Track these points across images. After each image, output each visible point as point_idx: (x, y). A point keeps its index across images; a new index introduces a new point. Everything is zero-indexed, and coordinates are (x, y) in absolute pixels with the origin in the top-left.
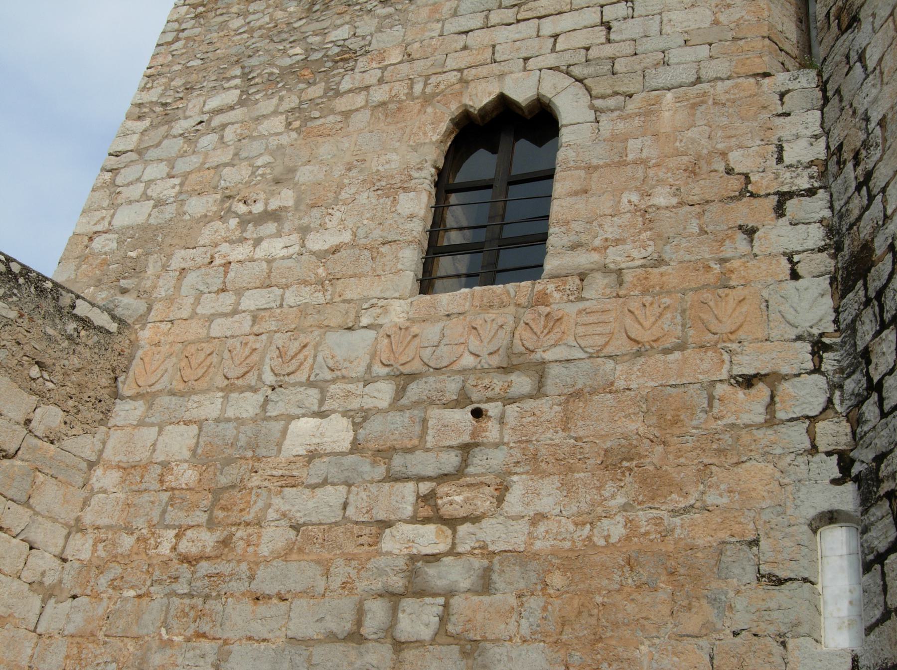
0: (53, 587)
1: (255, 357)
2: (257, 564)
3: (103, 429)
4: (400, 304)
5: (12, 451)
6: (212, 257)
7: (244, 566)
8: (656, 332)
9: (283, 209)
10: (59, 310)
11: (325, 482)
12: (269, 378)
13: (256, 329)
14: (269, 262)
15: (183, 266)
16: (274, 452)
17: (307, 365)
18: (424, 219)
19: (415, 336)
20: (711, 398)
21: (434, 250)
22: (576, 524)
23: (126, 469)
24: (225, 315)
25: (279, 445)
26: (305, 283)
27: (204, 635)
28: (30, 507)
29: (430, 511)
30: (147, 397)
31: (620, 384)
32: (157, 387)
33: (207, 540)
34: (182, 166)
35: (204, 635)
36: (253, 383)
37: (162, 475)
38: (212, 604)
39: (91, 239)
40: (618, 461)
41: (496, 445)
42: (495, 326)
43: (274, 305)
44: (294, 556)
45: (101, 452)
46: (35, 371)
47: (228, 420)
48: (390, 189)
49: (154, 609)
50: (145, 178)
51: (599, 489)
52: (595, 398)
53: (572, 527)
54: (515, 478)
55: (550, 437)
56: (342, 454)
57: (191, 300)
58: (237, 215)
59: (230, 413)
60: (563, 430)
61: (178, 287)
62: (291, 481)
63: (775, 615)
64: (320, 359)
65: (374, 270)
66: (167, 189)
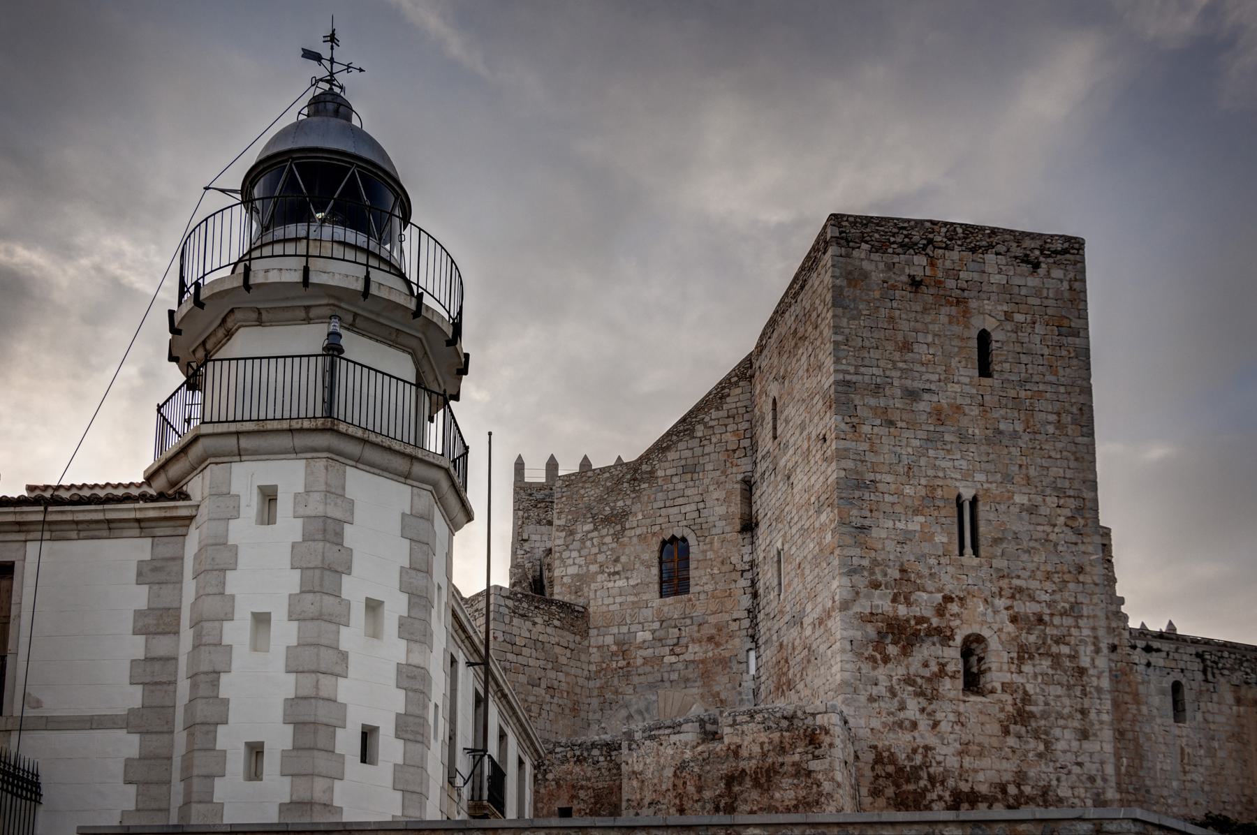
4: (657, 602)
21: (661, 582)
29: (672, 653)
30: (598, 628)
33: (622, 663)
40: (711, 639)
48: (649, 567)
55: (696, 635)
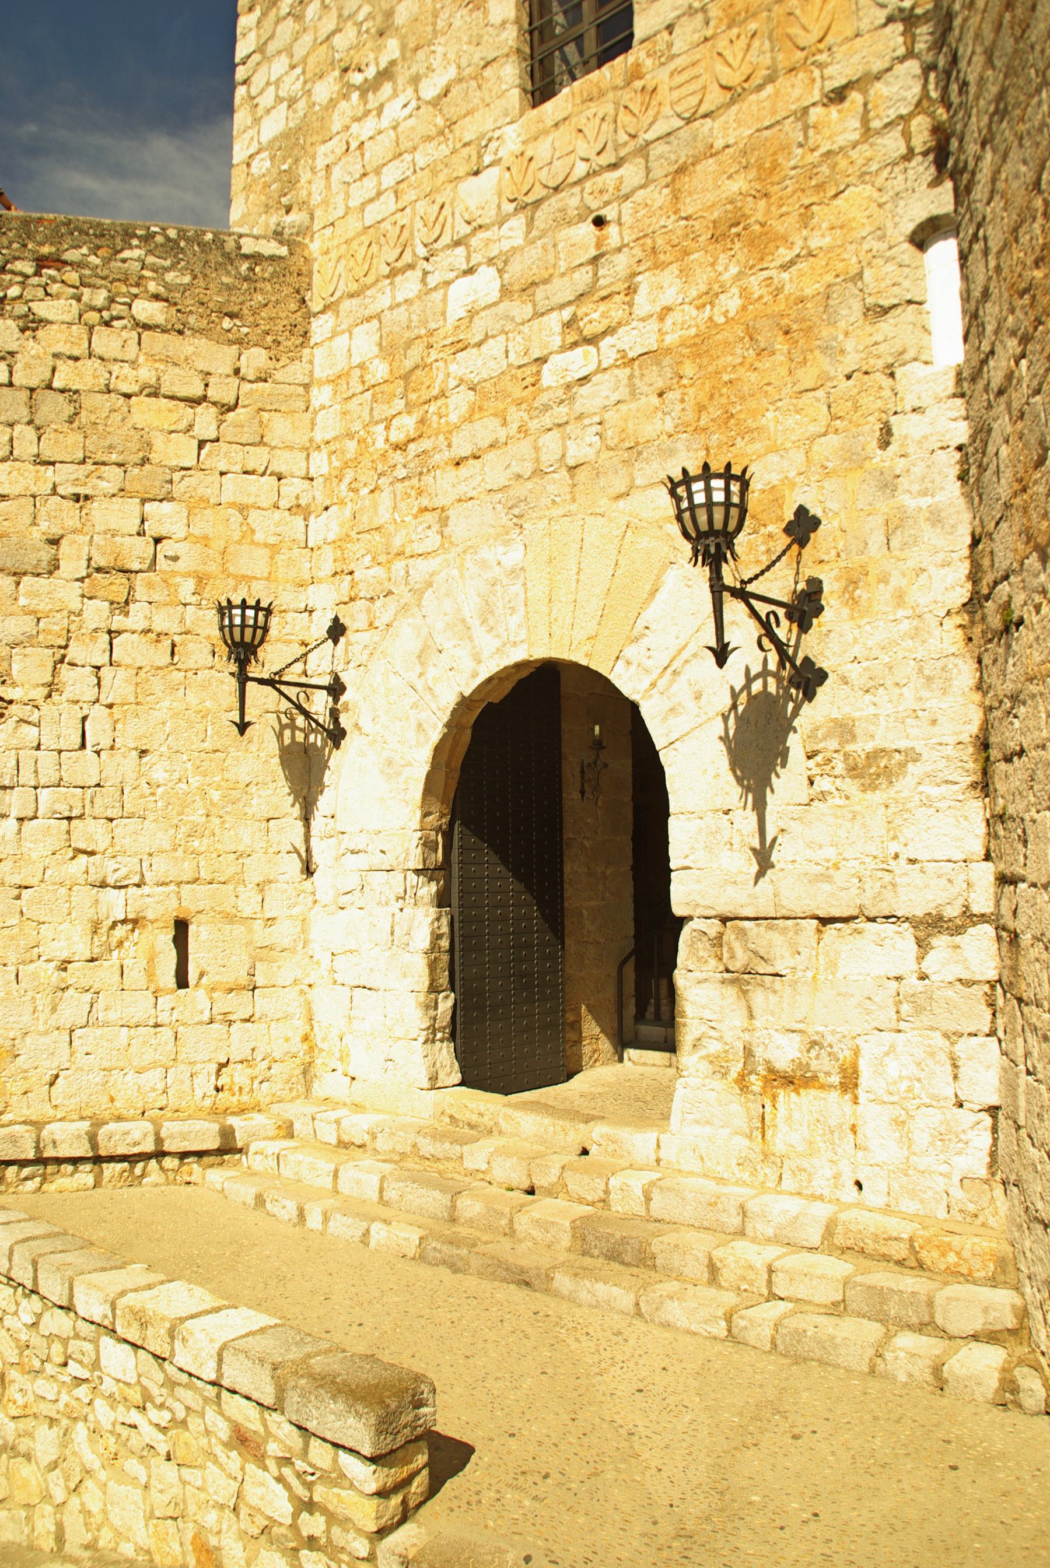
0: (308, 506)
1: (406, 234)
2: (450, 433)
3: (306, 351)
5: (232, 402)
6: (348, 143)
7: (441, 437)
8: (746, 70)
9: (393, 63)
10: (227, 256)
11: (487, 337)
12: (422, 252)
13: (400, 206)
14: (395, 128)
15: (327, 162)
16: (441, 323)
17: (448, 225)
18: (517, 21)
19: (531, 159)
20: (806, 129)
22: (698, 308)
23: (334, 381)
24: (371, 200)
25: (444, 314)
26: (429, 139)
27: (426, 509)
28: (265, 445)
31: (719, 144)
32: (338, 294)
34: (299, 51)
35: (426, 509)
36: (410, 261)
37: (362, 377)
38: (428, 479)
39: (248, 165)
40: (729, 229)
41: (619, 250)
42: (598, 121)
43: (408, 173)
44: (477, 416)
45: (312, 372)
46: (227, 323)
47: (398, 305)
49: (385, 498)
50: (273, 79)
51: (713, 264)
52: (698, 167)
53: (694, 313)
54: (639, 278)
56: (495, 304)
57: (342, 196)
58: (358, 88)
59: (400, 299)
60: (675, 213)
61: (328, 187)
62: (461, 345)
63: (882, 348)
64: (457, 215)
65: (483, 100)
66: (292, 85)
